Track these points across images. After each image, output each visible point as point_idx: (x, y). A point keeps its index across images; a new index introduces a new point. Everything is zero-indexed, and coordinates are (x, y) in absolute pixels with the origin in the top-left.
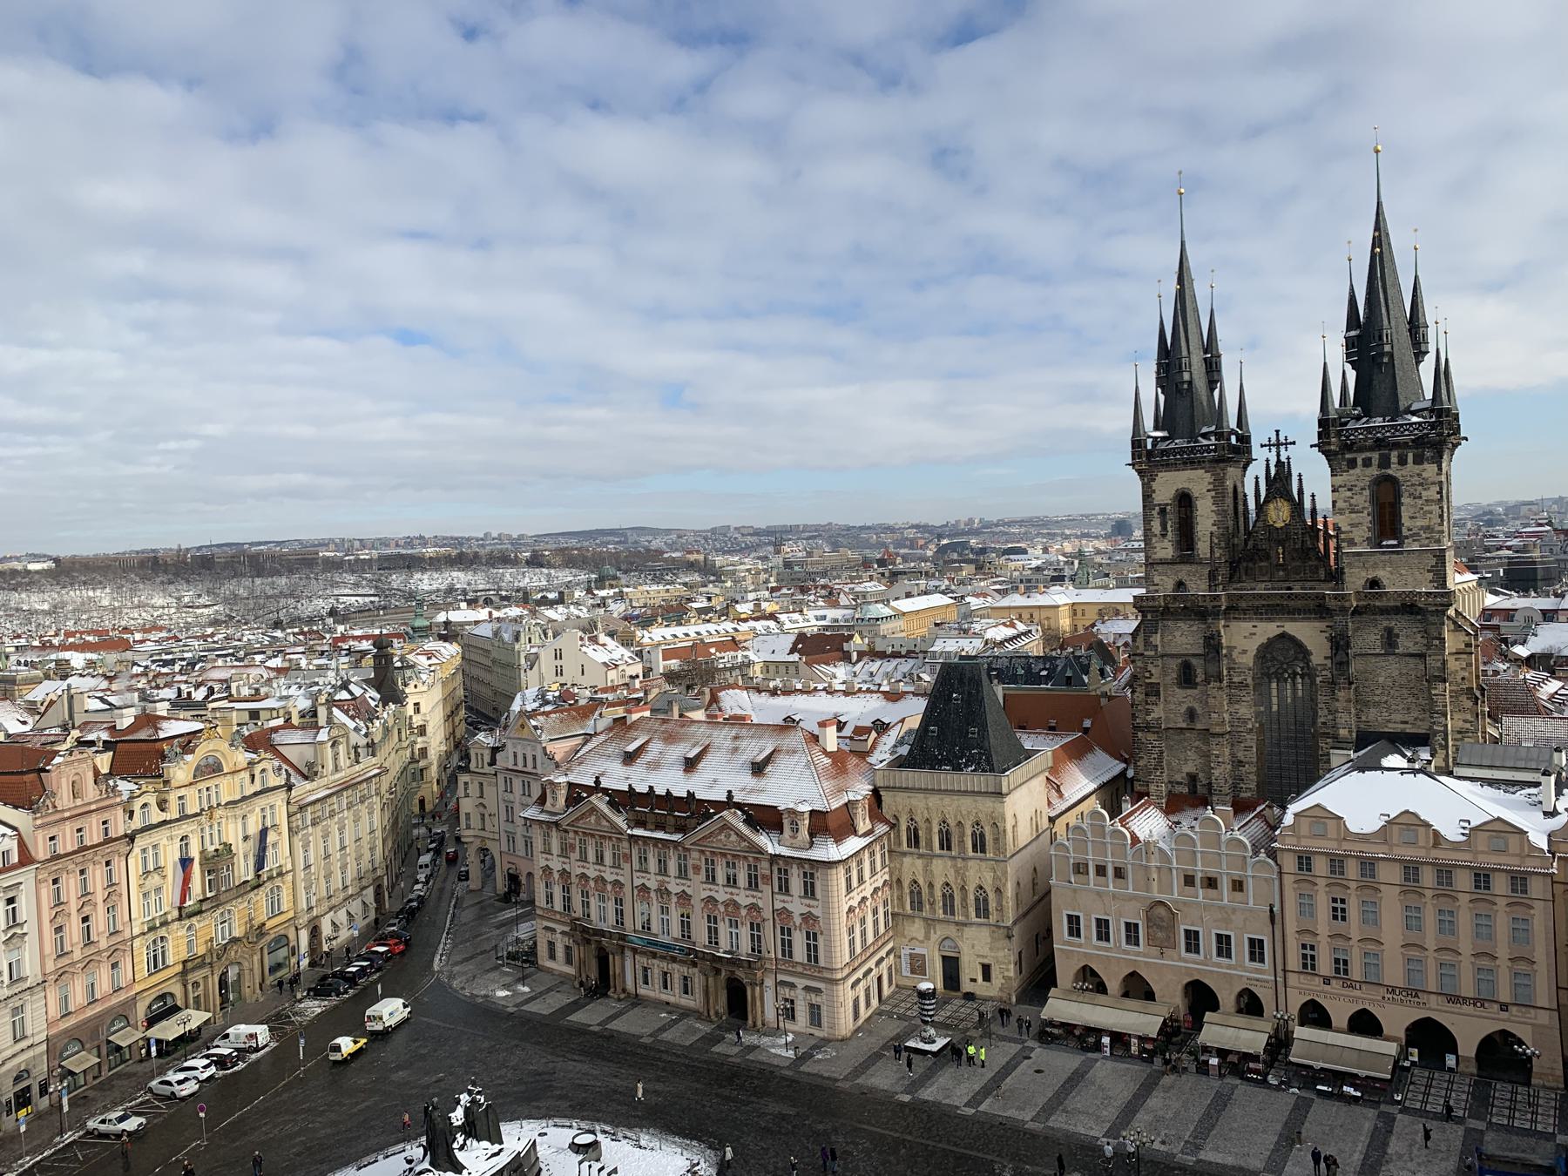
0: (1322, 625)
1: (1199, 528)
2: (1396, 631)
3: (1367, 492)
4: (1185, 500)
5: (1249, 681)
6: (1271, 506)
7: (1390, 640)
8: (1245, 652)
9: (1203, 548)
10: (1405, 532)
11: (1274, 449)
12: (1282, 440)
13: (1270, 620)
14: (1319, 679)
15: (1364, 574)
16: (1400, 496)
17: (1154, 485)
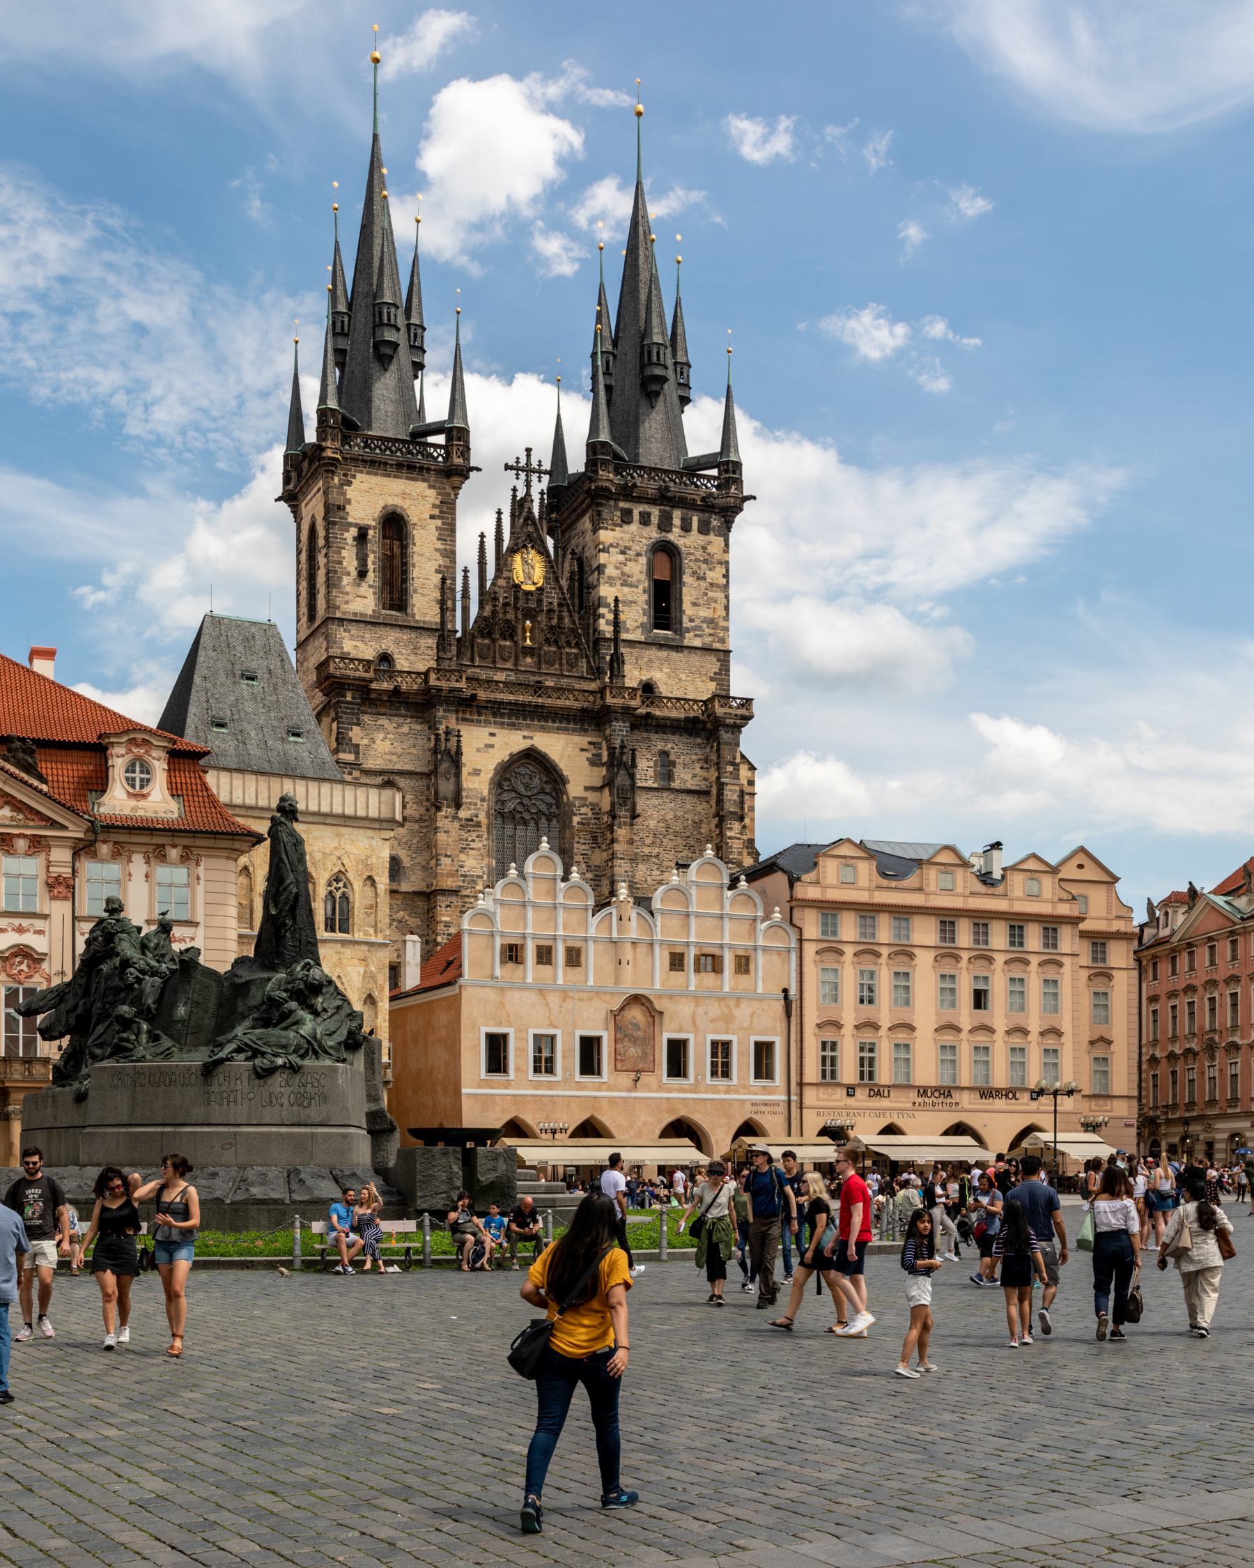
0: (583, 740)
1: (416, 573)
2: (672, 758)
3: (643, 560)
4: (394, 525)
5: (482, 818)
6: (518, 558)
7: (666, 767)
8: (477, 772)
9: (424, 606)
10: (686, 623)
11: (523, 475)
12: (534, 464)
13: (513, 726)
14: (576, 819)
15: (636, 673)
16: (681, 573)
17: (350, 492)
